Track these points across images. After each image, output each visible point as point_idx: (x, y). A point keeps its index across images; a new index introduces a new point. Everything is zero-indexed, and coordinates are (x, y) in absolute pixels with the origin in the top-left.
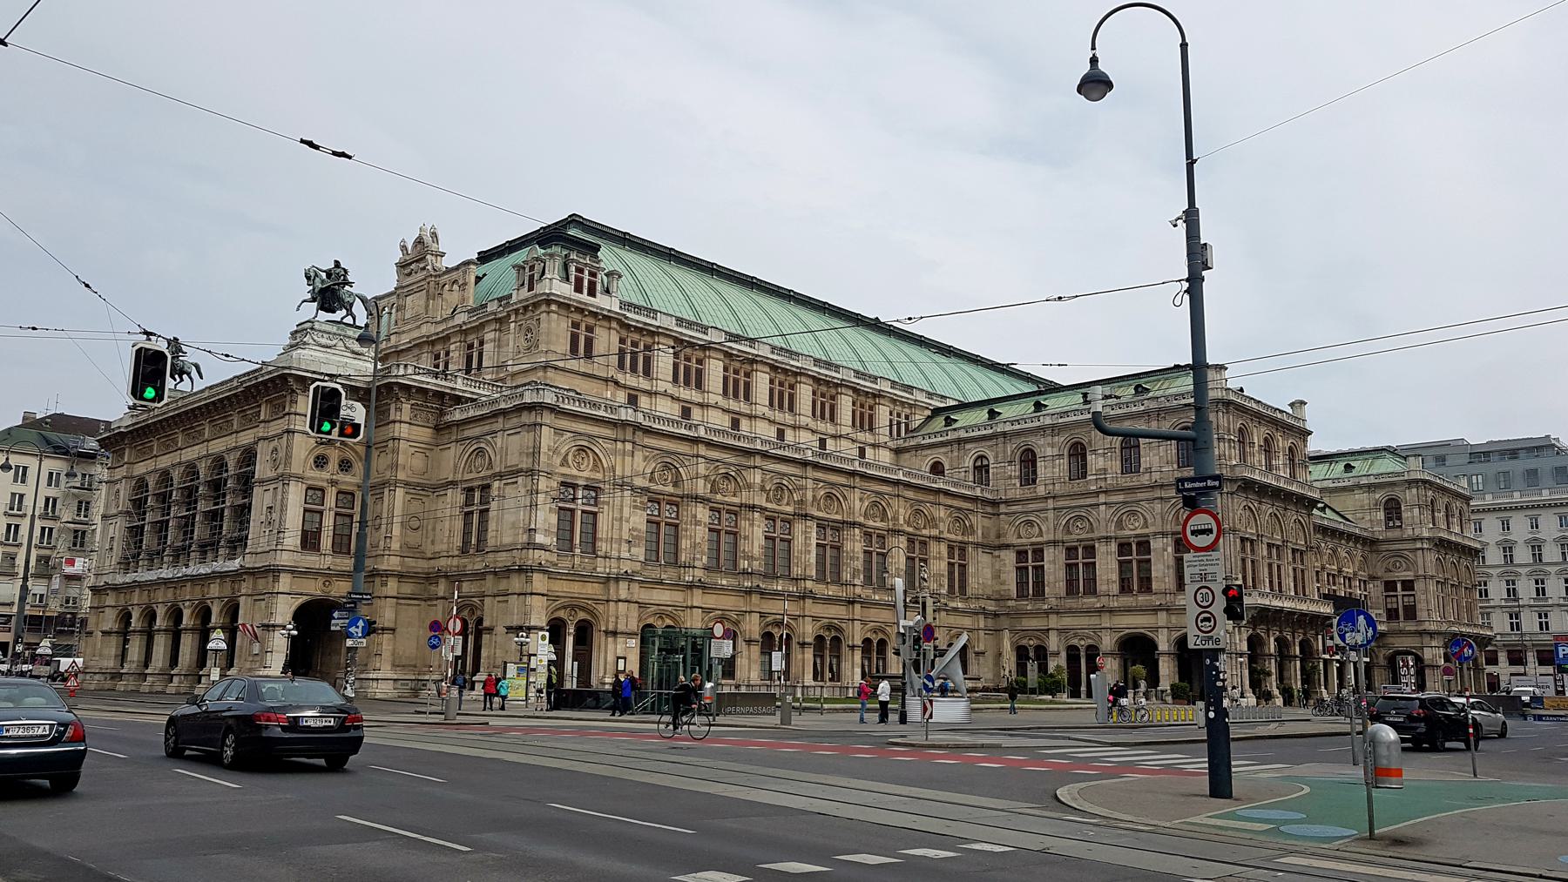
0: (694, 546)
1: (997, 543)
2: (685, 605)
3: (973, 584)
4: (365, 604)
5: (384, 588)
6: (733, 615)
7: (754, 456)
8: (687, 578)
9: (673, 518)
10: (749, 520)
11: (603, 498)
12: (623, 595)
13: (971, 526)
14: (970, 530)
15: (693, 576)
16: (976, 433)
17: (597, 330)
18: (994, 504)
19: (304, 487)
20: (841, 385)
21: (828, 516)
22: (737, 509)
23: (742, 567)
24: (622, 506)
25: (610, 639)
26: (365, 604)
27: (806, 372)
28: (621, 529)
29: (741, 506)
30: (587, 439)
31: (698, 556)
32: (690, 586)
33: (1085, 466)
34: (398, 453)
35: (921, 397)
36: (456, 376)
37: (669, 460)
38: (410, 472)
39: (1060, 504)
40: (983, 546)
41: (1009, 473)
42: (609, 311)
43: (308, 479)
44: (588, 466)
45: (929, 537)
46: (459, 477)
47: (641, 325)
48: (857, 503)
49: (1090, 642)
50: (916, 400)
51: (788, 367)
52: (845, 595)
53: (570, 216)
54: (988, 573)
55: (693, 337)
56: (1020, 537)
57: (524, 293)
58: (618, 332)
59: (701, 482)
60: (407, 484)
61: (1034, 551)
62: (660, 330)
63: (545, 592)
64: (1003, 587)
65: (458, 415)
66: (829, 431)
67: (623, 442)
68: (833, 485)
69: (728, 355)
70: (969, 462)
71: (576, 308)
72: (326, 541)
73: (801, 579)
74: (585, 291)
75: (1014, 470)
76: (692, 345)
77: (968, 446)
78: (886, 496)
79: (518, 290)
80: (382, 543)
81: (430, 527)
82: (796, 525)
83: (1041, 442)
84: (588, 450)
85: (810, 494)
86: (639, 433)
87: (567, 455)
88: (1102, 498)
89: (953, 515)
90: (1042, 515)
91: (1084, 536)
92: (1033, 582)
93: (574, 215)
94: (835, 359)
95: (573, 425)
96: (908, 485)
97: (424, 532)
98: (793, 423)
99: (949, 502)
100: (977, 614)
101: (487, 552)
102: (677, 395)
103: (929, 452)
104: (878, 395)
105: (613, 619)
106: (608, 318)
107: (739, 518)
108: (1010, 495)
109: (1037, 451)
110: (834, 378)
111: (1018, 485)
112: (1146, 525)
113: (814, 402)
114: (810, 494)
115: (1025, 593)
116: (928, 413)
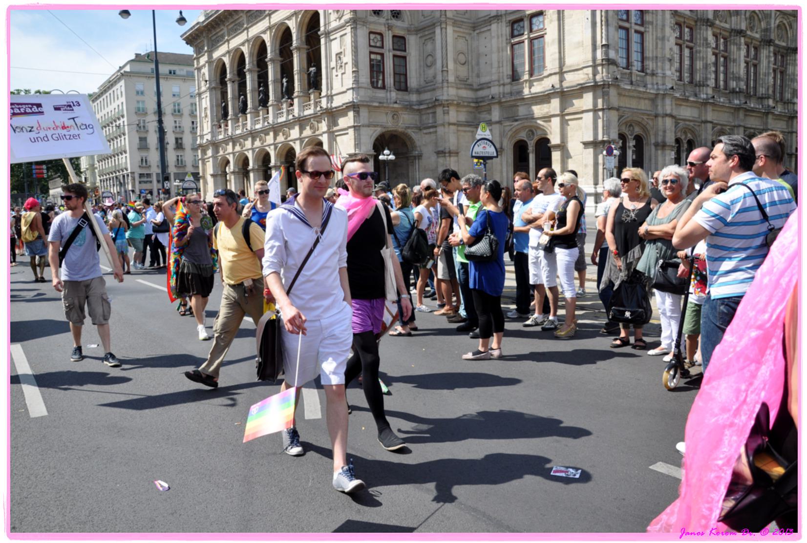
0: (706, 66)
2: (700, 120)
4: (426, 134)
5: (446, 117)
10: (737, 44)
15: (707, 94)
22: (727, 34)
23: (731, 87)
24: (663, 26)
25: (660, 152)
26: (426, 134)
28: (663, 48)
29: (732, 30)
31: (709, 76)
32: (705, 103)
43: (371, 23)
52: (787, 111)
72: (390, 80)
73: (765, 98)
80: (439, 78)
81: (474, 63)
101: (551, 75)
105: (661, 133)
107: (728, 43)
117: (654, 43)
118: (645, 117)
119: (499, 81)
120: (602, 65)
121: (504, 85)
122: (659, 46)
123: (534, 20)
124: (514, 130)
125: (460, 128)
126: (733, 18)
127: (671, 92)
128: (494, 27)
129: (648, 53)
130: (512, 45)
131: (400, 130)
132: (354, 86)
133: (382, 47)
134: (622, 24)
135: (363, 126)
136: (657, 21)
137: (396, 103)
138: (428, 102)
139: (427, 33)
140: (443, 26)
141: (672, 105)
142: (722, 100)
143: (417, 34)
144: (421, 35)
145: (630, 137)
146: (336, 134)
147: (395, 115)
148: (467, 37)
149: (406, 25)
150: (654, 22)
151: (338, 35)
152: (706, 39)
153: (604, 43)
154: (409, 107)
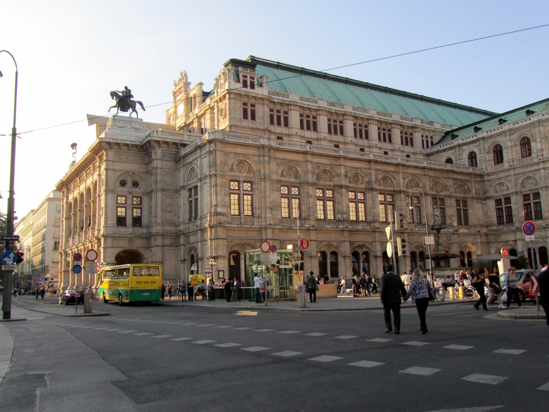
0: (309, 208)
1: (484, 196)
3: (472, 219)
6: (335, 244)
7: (340, 159)
8: (306, 226)
9: (297, 195)
10: (340, 193)
11: (254, 186)
12: (270, 236)
13: (469, 189)
14: (469, 191)
15: (310, 224)
16: (468, 140)
17: (257, 106)
18: (481, 176)
19: (116, 196)
20: (393, 123)
21: (386, 188)
23: (337, 218)
24: (265, 190)
27: (373, 118)
28: (265, 202)
29: (335, 186)
30: (243, 156)
31: (311, 214)
32: (309, 230)
33: (530, 150)
34: (157, 175)
35: (437, 126)
36: (184, 135)
37: (291, 165)
38: (164, 184)
39: (517, 172)
40: (477, 199)
41: (488, 159)
42: (262, 95)
44: (245, 171)
45: (445, 196)
46: (186, 184)
47: (280, 101)
48: (402, 181)
49: (541, 245)
50: (435, 128)
51: (363, 116)
53: (249, 57)
54: (480, 213)
55: (309, 105)
56: (496, 192)
58: (268, 105)
59: (310, 175)
60: (163, 190)
62: (291, 103)
63: (225, 237)
64: (489, 220)
65: (183, 152)
66: (389, 147)
67: (264, 156)
68: (386, 172)
69: (331, 113)
70: (465, 156)
71: (245, 95)
73: (372, 222)
74: (249, 87)
75: (491, 156)
76: (310, 109)
77: (464, 147)
78: (418, 176)
82: (367, 194)
83: (504, 139)
84: (245, 163)
85: (373, 179)
86: (272, 152)
87: (233, 165)
88: (541, 166)
89: (458, 183)
91: (533, 187)
92: (506, 215)
93: (251, 56)
94: (390, 111)
95: (235, 149)
96: (430, 169)
97: (174, 213)
98: (368, 145)
99: (455, 176)
100: (476, 234)
102: (303, 135)
103: (442, 154)
104: (414, 127)
106: (262, 99)
108: (489, 170)
109: (502, 144)
110: (389, 120)
111: (493, 164)
113: (379, 134)
114: (373, 179)
115: (502, 222)
116: (443, 134)
117: (260, 200)
118: (251, 241)
119: (183, 222)
122: (263, 201)
124: (189, 249)
125: (165, 248)
126: (335, 179)
127: (270, 226)
128: (182, 192)
129: (254, 206)
131: (134, 249)
133: (126, 204)
134: (231, 191)
135: (109, 247)
136: (261, 188)
137: (130, 234)
140: (155, 192)
141: (273, 233)
142: (328, 226)
145: (241, 252)
147: (131, 240)
148: (173, 197)
149: (142, 190)
150: (259, 188)
152: (308, 193)
154: (140, 237)
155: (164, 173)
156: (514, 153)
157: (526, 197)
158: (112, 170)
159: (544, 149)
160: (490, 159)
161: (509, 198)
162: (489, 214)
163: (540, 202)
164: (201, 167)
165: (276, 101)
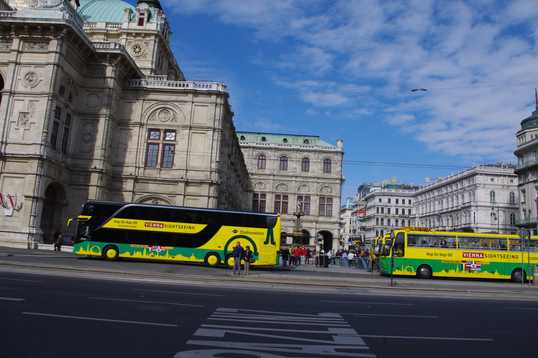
4: (75, 189)
17: (164, 59)
26: (75, 189)
34: (112, 99)
46: (144, 121)
47: (171, 62)
57: (134, 25)
61: (262, 195)
64: (247, 207)
67: (228, 123)
79: (129, 23)
88: (294, 179)
90: (267, 181)
91: (284, 192)
108: (253, 172)
111: (257, 168)
112: (309, 191)
120: (216, 172)
121: (139, 168)
123: (168, 134)
124: (143, 198)
130: (148, 144)
132: (43, 143)
133: (59, 119)
138: (82, 166)
139: (89, 118)
143: (79, 116)
144: (84, 118)
146: (6, 175)
148: (114, 130)
151: (27, 99)
153: (217, 160)
155: (115, 98)
156: (275, 165)
157: (278, 196)
158: (62, 68)
159: (298, 169)
160: (256, 163)
161: (265, 195)
162: (248, 203)
163: (287, 203)
164: (192, 114)
165: (170, 60)
